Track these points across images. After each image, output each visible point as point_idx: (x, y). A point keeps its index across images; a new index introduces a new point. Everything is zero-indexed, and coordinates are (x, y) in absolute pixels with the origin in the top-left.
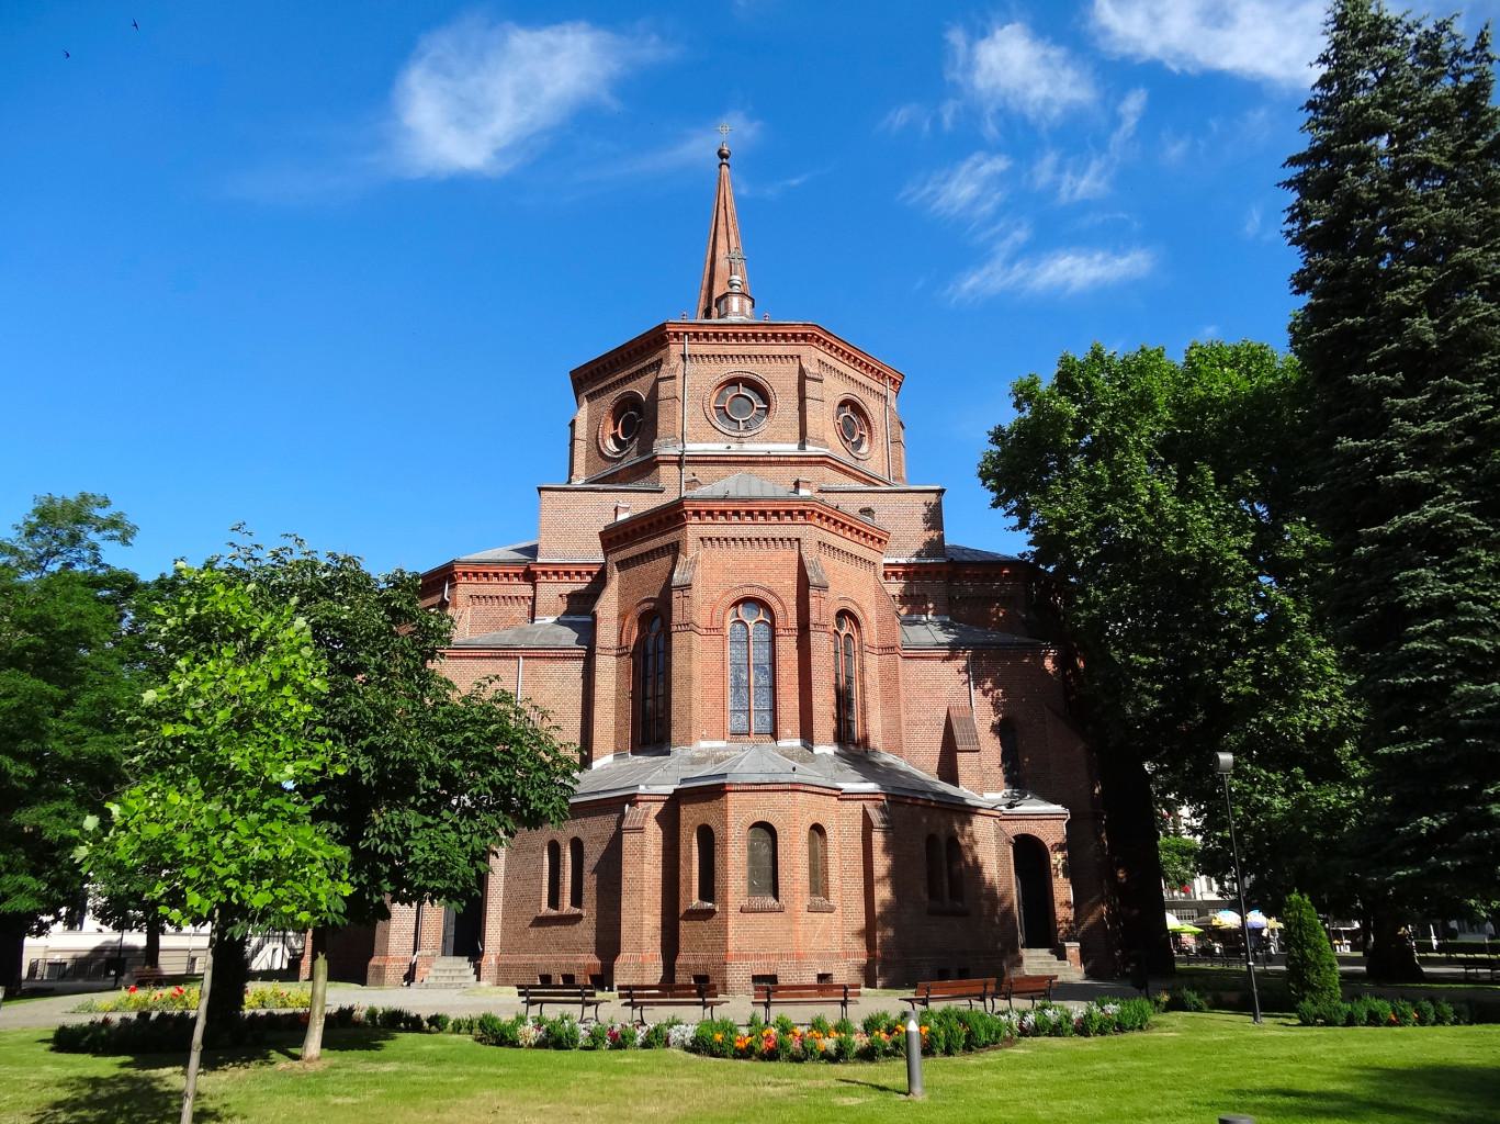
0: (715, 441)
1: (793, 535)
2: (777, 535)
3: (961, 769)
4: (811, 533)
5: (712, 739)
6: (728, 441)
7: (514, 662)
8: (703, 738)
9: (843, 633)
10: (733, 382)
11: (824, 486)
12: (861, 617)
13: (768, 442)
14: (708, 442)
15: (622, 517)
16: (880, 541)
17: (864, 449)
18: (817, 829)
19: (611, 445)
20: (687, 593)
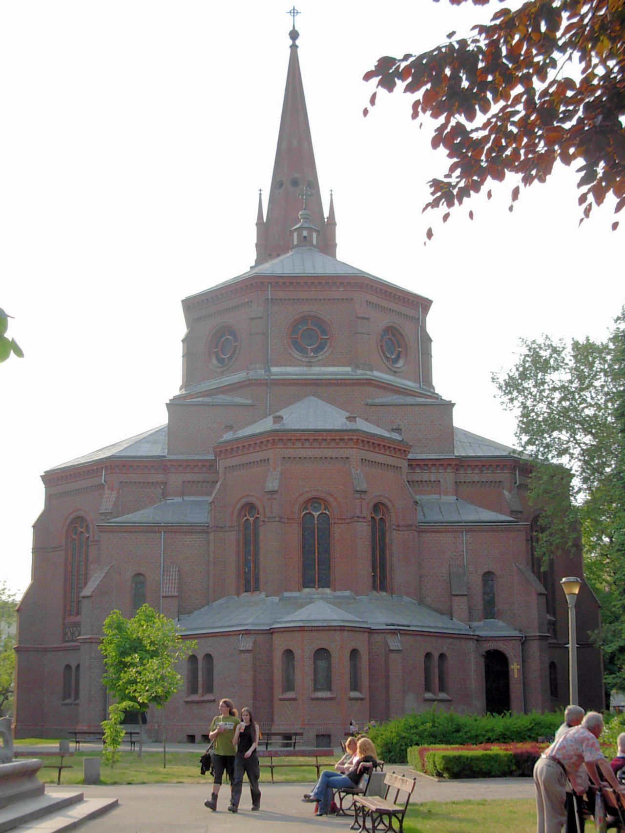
0: (290, 366)
1: (344, 456)
2: (334, 456)
3: (455, 607)
4: (355, 453)
5: (291, 591)
6: (301, 365)
7: (158, 535)
8: (286, 591)
9: (377, 518)
10: (304, 319)
11: (370, 401)
12: (389, 505)
13: (330, 366)
14: (286, 366)
15: (228, 436)
16: (405, 451)
17: (401, 363)
18: (354, 653)
19: (214, 361)
20: (275, 496)
